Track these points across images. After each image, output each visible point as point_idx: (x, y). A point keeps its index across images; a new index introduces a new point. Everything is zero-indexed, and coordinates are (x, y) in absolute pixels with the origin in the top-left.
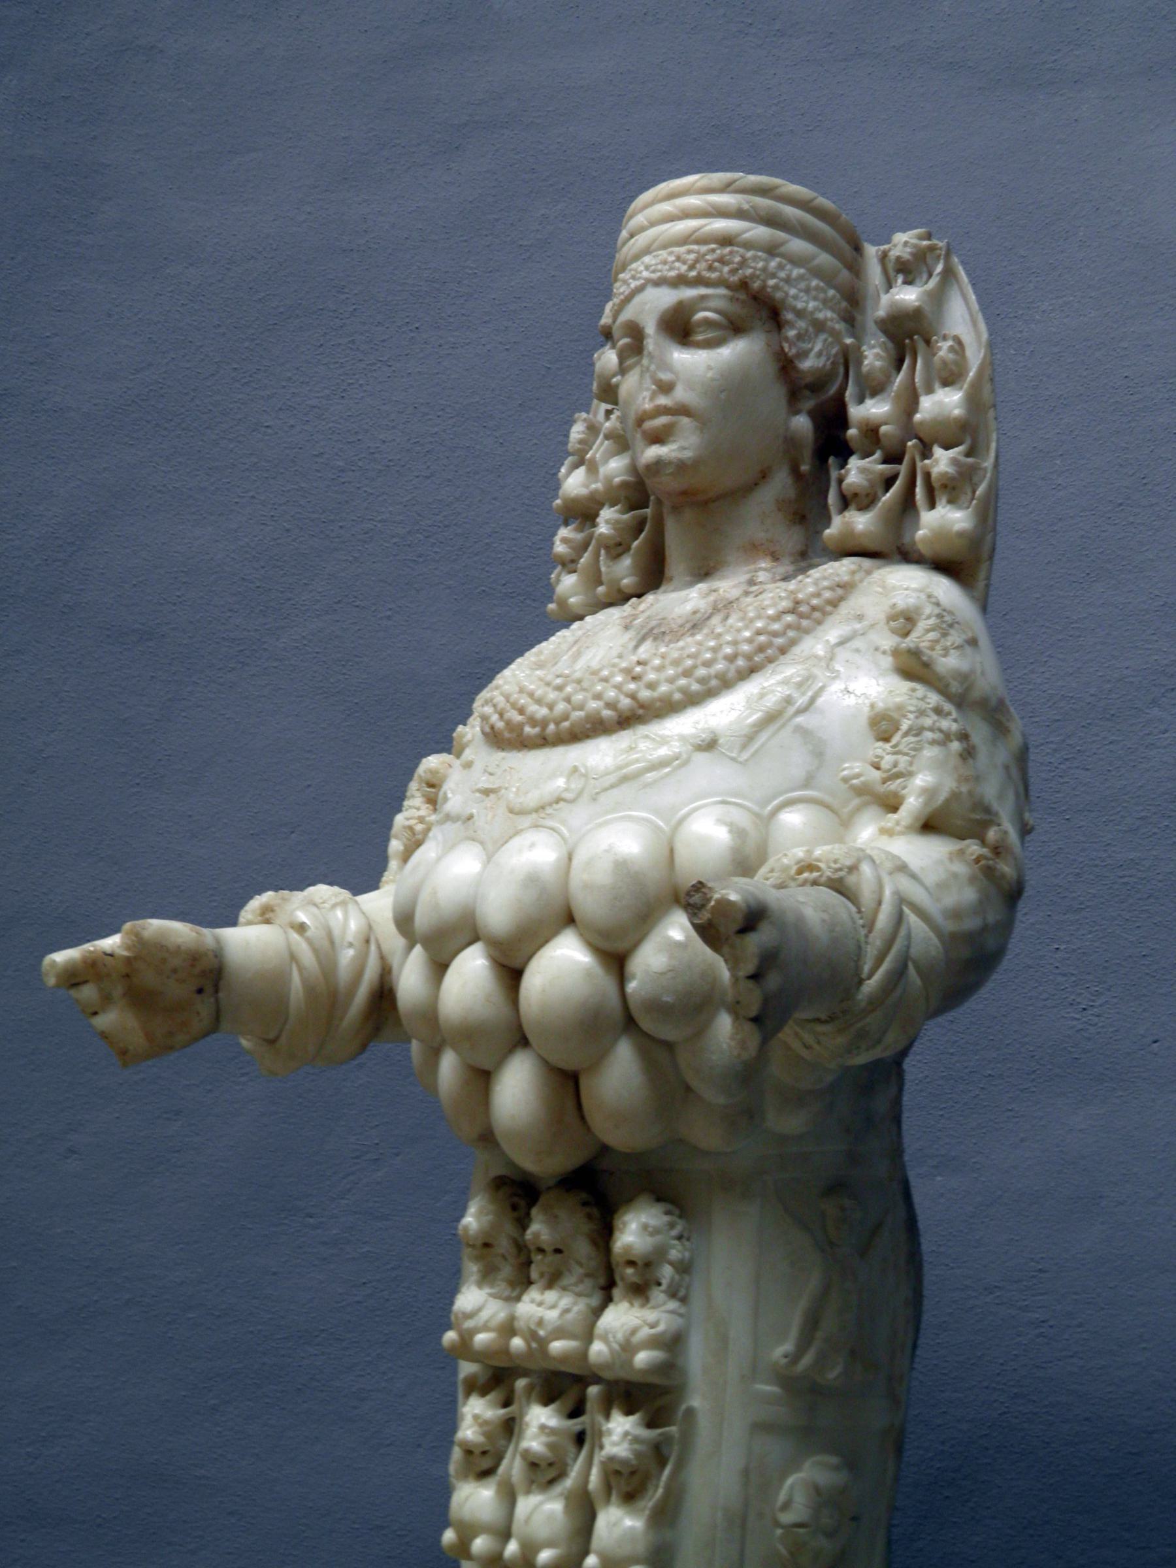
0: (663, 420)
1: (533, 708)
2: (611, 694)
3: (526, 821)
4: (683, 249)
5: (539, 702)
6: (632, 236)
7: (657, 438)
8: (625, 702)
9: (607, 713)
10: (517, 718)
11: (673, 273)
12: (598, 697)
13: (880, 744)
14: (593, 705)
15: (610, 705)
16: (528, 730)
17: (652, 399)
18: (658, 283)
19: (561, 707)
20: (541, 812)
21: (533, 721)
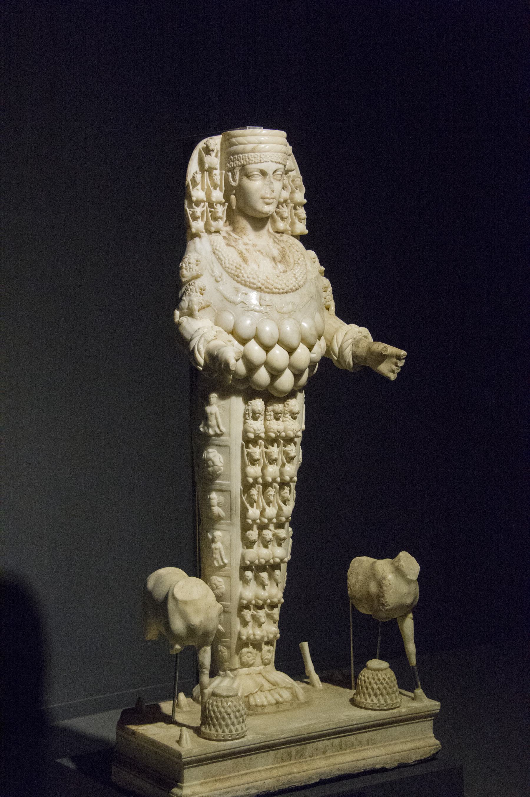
0: (271, 201)
1: (275, 285)
2: (294, 284)
3: (286, 316)
4: (279, 154)
5: (277, 283)
6: (261, 143)
7: (268, 204)
8: (297, 286)
9: (294, 288)
10: (270, 287)
11: (277, 161)
12: (292, 284)
13: (324, 293)
14: (291, 286)
15: (295, 286)
16: (274, 290)
17: (271, 194)
18: (272, 162)
19: (284, 286)
20: (290, 314)
21: (276, 288)
